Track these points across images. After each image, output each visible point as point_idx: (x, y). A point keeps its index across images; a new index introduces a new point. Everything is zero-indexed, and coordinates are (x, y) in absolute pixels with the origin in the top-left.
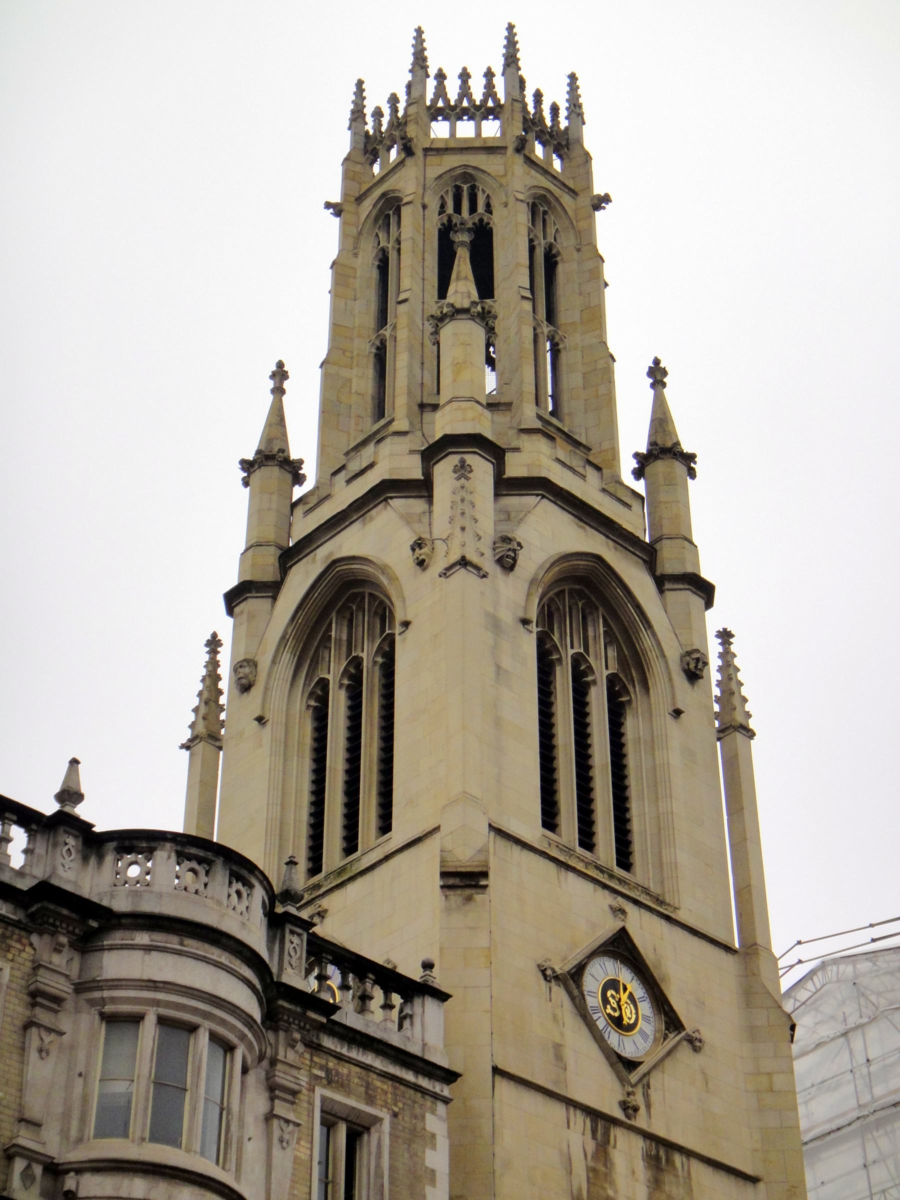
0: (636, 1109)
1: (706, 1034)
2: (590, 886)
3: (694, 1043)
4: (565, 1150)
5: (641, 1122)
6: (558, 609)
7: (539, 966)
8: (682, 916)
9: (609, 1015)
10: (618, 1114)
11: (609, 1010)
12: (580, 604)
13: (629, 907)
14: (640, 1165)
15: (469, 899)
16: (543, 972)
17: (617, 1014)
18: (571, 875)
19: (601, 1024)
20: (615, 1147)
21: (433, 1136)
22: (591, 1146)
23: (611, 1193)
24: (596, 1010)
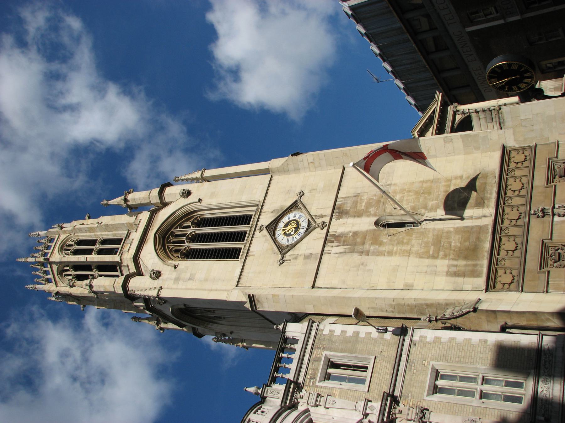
0: (324, 223)
1: (298, 191)
2: (254, 241)
3: (302, 194)
4: (337, 255)
5: (327, 220)
6: (174, 248)
7: (280, 265)
8: (262, 200)
9: (295, 233)
10: (325, 229)
11: (293, 233)
12: (172, 238)
13: (260, 224)
14: (342, 221)
15: (258, 301)
16: (281, 264)
17: (294, 229)
18: (251, 249)
19: (298, 237)
20: (336, 232)
21: (330, 331)
23: (351, 234)
24: (293, 240)
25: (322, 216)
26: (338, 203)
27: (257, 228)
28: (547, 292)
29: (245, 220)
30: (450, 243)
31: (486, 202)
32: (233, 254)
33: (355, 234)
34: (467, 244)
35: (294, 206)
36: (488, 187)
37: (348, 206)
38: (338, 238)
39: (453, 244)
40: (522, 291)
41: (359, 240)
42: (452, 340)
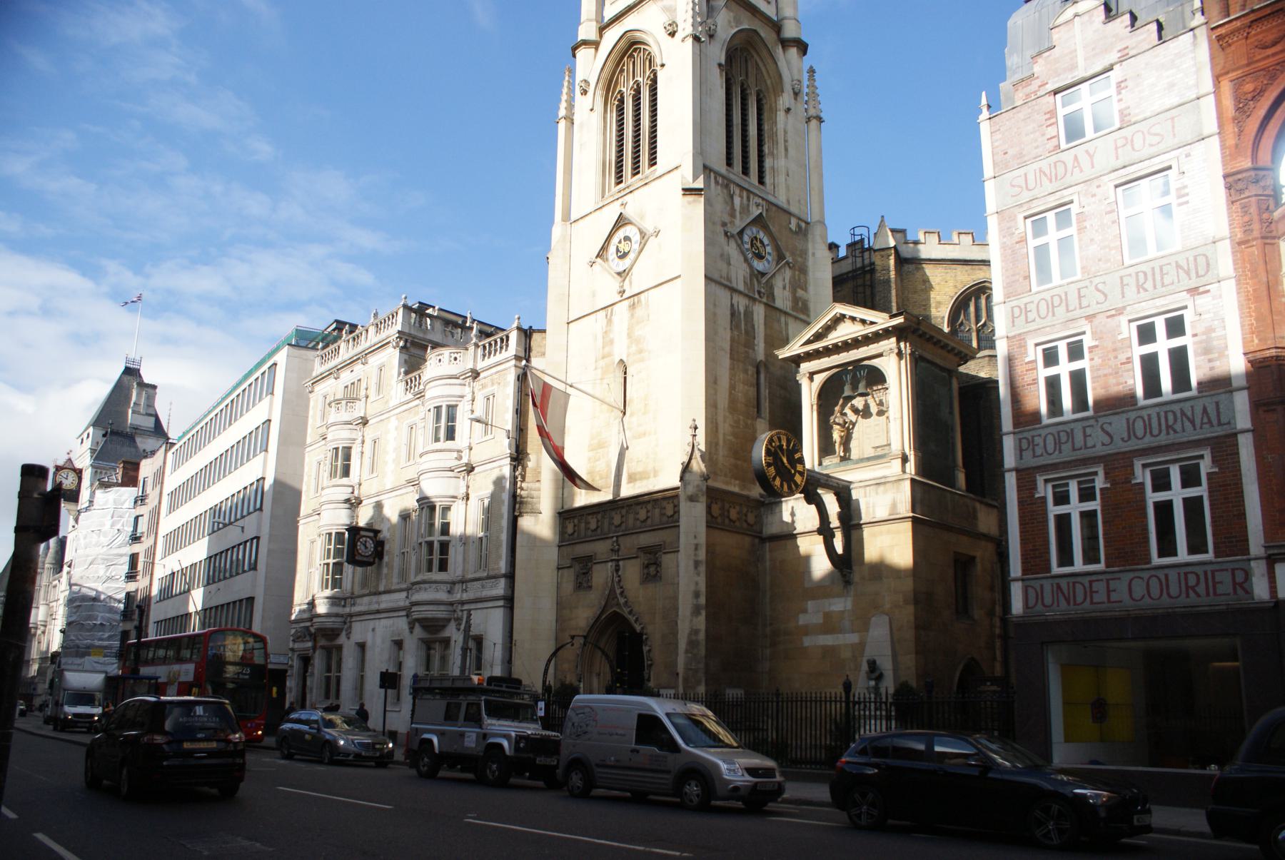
10: (618, 298)
22: (605, 321)
25: (631, 283)
26: (642, 296)
27: (620, 200)
28: (558, 569)
29: (653, 161)
30: (599, 460)
31: (632, 485)
32: (619, 179)
33: (612, 342)
34: (598, 478)
35: (643, 234)
36: (645, 482)
37: (639, 312)
38: (610, 321)
39: (598, 463)
40: (559, 546)
41: (607, 349)
42: (503, 502)
